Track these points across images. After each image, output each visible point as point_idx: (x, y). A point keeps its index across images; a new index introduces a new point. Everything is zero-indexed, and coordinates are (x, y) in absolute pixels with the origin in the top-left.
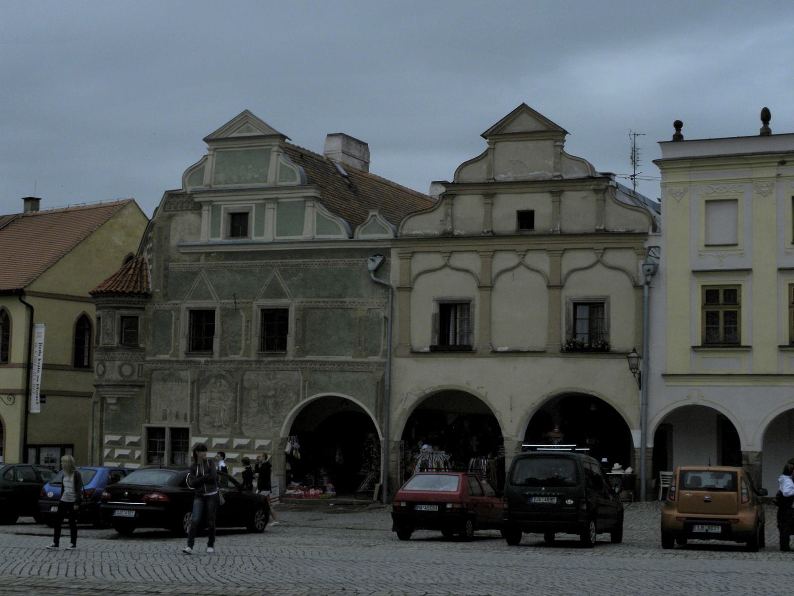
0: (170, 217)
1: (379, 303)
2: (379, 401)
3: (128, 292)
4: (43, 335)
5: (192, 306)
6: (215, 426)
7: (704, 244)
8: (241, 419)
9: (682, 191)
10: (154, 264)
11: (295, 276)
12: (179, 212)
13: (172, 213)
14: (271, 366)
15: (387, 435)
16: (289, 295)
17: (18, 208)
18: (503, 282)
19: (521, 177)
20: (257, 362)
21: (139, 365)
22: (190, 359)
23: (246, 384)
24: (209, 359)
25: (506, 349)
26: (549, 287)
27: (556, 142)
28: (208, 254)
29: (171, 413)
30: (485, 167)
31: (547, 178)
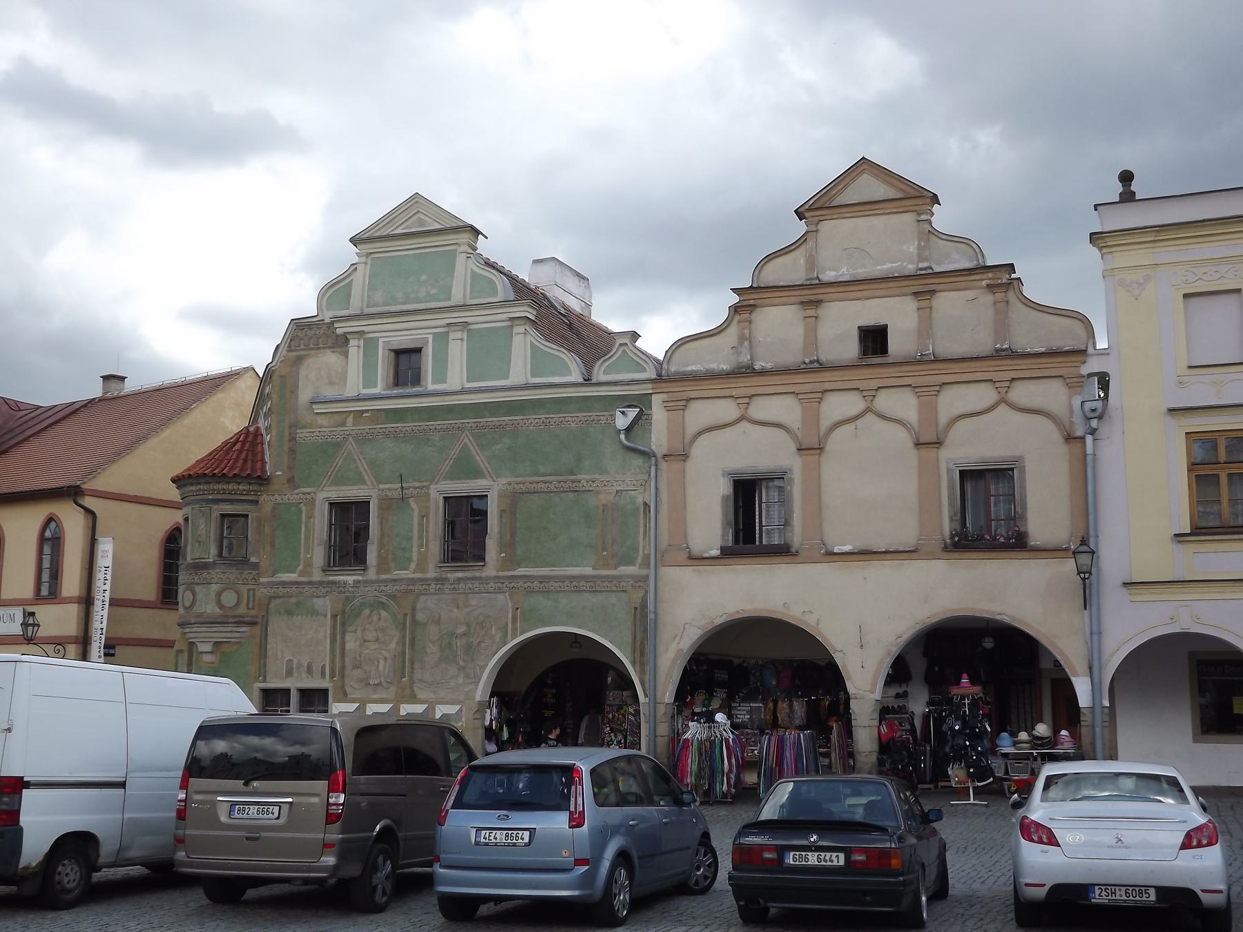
0: (299, 360)
1: (635, 483)
2: (638, 639)
3: (231, 475)
4: (110, 554)
6: (369, 684)
7: (1186, 364)
9: (1142, 281)
10: (274, 433)
11: (498, 444)
12: (313, 352)
13: (303, 353)
14: (460, 586)
15: (652, 693)
17: (95, 390)
19: (862, 272)
20: (438, 580)
21: (249, 590)
23: (420, 616)
24: (360, 578)
25: (847, 548)
26: (918, 444)
27: (919, 214)
29: (300, 666)
30: (802, 261)
31: (906, 273)
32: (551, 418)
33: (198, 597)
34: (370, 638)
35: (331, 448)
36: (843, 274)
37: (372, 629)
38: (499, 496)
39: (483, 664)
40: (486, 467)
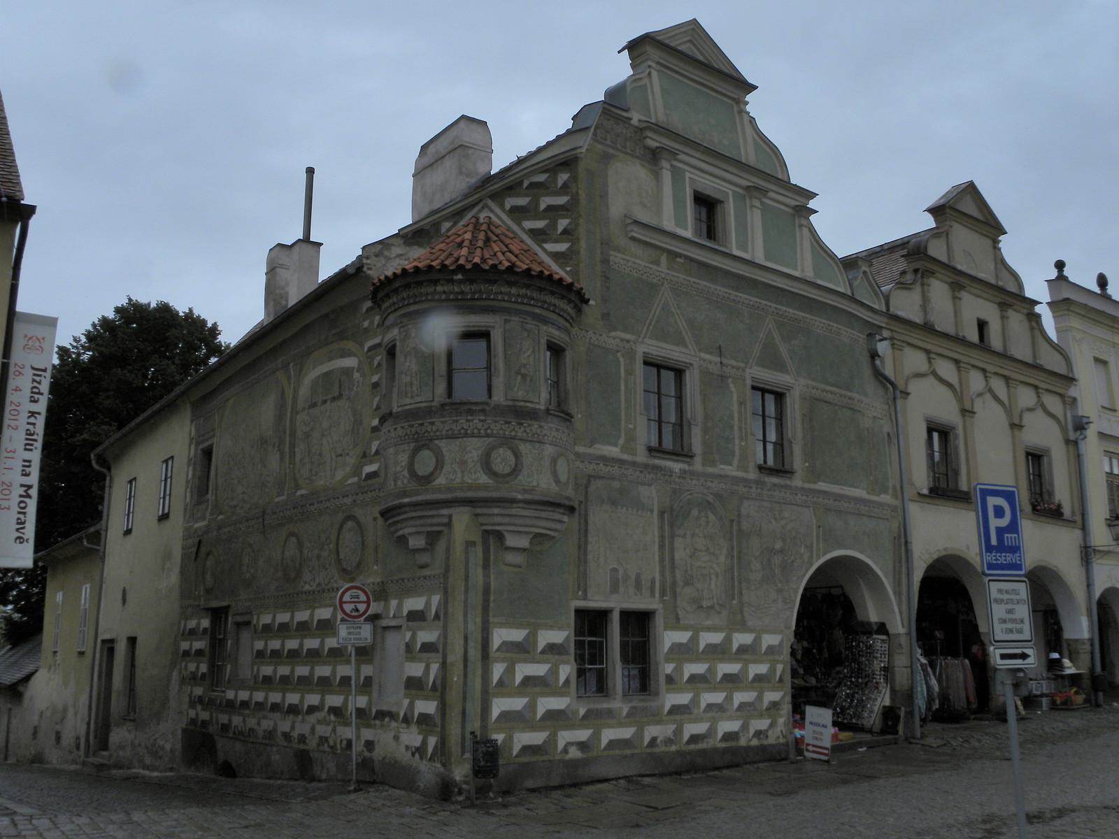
0: (606, 158)
5: (655, 353)
6: (702, 607)
12: (621, 155)
13: (611, 151)
20: (759, 483)
24: (686, 467)
28: (673, 255)
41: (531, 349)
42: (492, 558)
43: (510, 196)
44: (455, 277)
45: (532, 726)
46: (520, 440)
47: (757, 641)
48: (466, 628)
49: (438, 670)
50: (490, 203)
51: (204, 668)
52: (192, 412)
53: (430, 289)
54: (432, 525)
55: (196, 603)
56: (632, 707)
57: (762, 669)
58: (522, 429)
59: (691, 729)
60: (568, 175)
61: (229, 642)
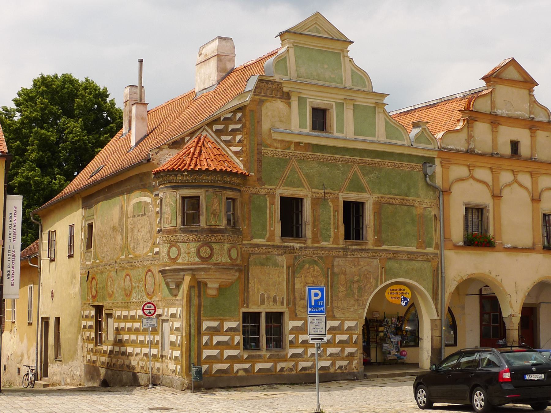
0: (261, 102)
2: (435, 286)
8: (332, 302)
12: (269, 99)
13: (263, 98)
14: (356, 253)
16: (368, 190)
18: (506, 193)
22: (286, 244)
23: (336, 270)
24: (302, 245)
25: (509, 246)
28: (297, 144)
29: (269, 297)
30: (489, 102)
32: (397, 163)
33: (215, 252)
34: (309, 282)
35: (283, 162)
36: (503, 113)
37: (310, 276)
38: (373, 204)
39: (366, 298)
40: (366, 186)
41: (218, 203)
42: (202, 292)
43: (215, 124)
44: (184, 174)
45: (222, 362)
46: (213, 242)
47: (342, 324)
48: (190, 322)
49: (180, 338)
50: (206, 127)
51: (93, 335)
52: (82, 203)
53: (175, 178)
54: (177, 279)
55: (88, 303)
56: (271, 354)
57: (345, 337)
58: (214, 238)
59: (302, 365)
60: (241, 114)
61: (104, 322)
